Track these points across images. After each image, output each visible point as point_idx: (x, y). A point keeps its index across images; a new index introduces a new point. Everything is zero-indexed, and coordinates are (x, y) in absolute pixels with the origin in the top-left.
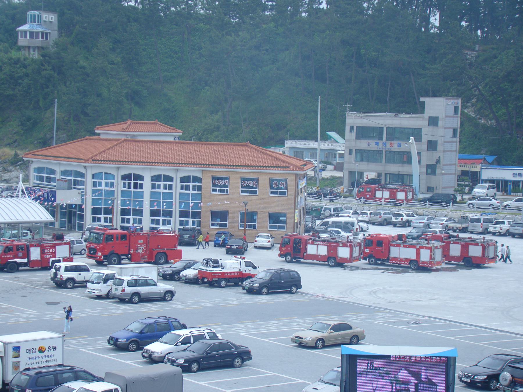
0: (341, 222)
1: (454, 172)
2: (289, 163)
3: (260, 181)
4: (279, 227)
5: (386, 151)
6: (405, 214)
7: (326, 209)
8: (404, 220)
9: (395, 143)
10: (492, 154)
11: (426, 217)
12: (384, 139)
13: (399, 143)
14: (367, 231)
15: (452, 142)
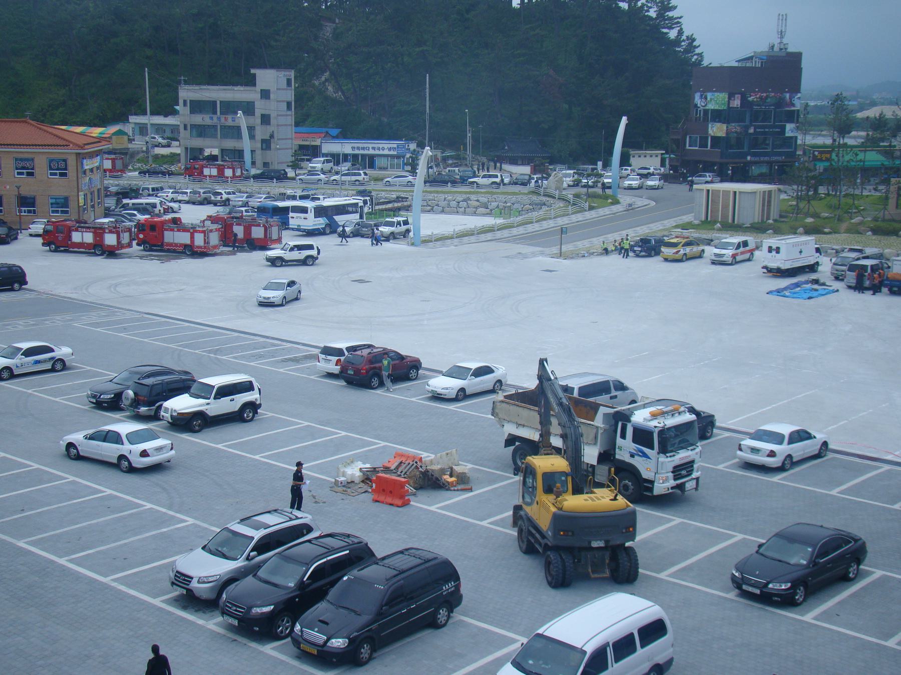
0: (142, 204)
1: (290, 146)
2: (71, 142)
3: (37, 161)
4: (63, 212)
5: (221, 126)
6: (225, 192)
7: (144, 189)
8: (223, 199)
9: (230, 117)
10: (337, 128)
11: (246, 195)
12: (218, 113)
13: (233, 118)
14: (180, 211)
15: (287, 115)
